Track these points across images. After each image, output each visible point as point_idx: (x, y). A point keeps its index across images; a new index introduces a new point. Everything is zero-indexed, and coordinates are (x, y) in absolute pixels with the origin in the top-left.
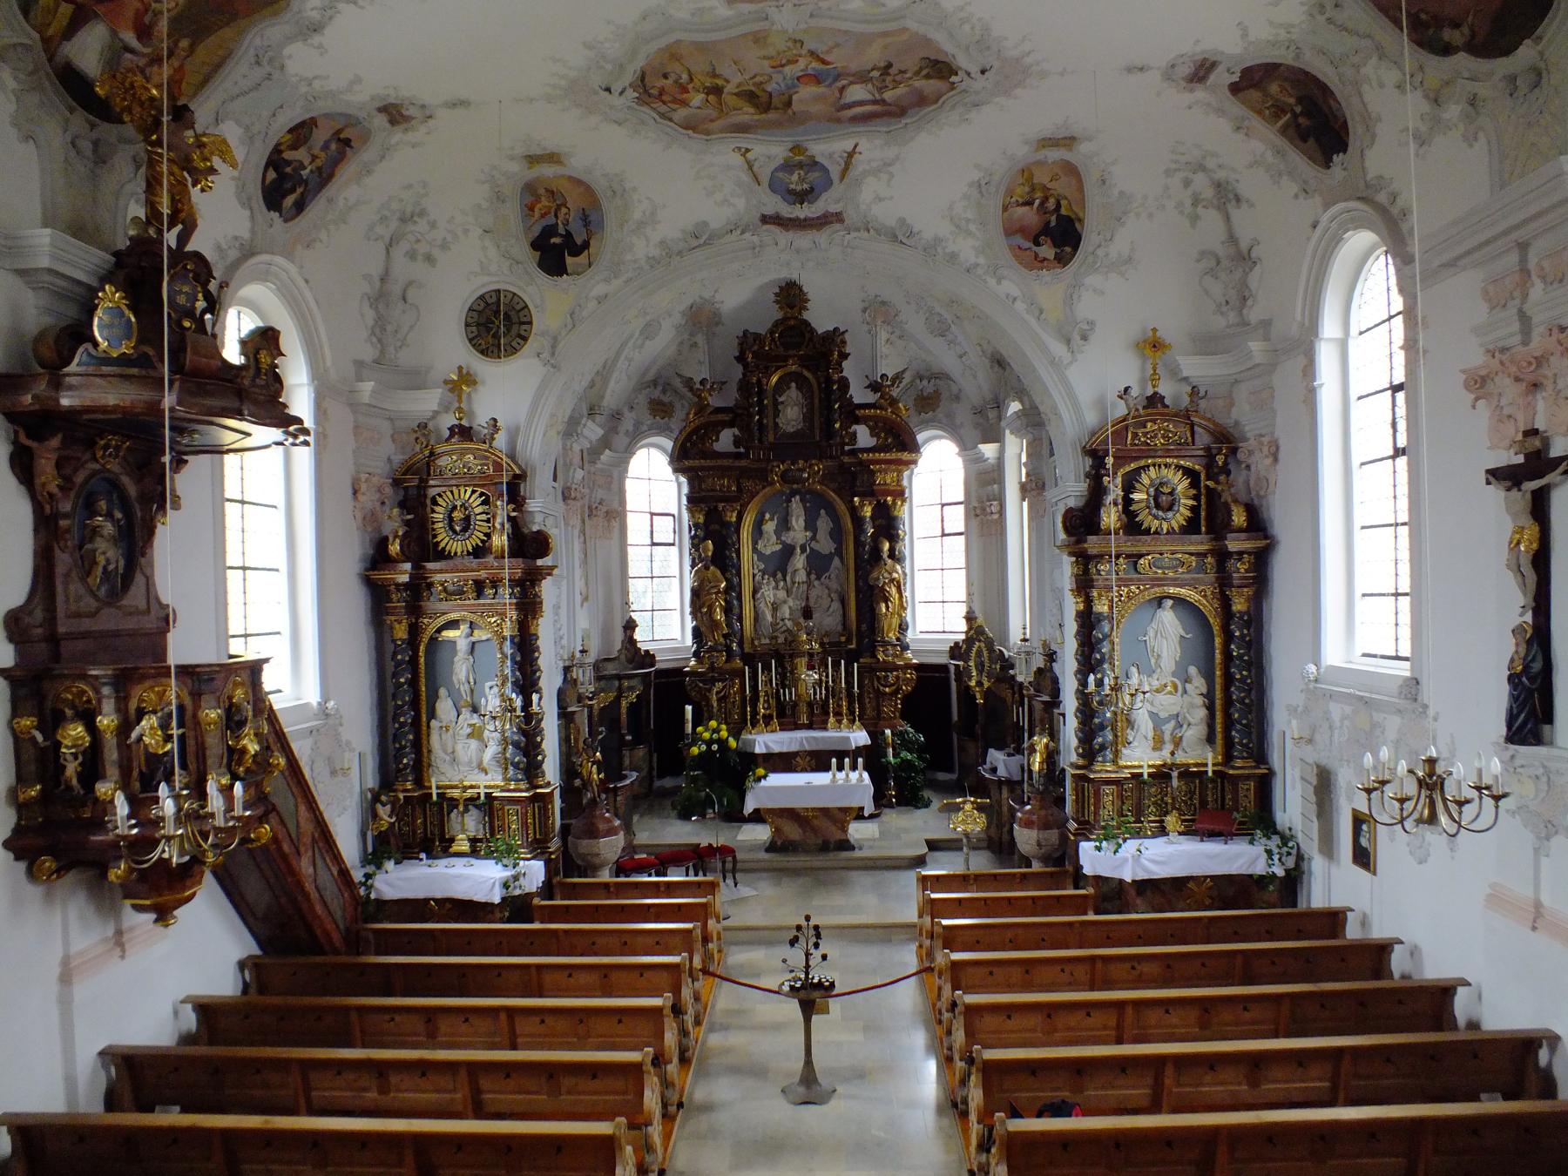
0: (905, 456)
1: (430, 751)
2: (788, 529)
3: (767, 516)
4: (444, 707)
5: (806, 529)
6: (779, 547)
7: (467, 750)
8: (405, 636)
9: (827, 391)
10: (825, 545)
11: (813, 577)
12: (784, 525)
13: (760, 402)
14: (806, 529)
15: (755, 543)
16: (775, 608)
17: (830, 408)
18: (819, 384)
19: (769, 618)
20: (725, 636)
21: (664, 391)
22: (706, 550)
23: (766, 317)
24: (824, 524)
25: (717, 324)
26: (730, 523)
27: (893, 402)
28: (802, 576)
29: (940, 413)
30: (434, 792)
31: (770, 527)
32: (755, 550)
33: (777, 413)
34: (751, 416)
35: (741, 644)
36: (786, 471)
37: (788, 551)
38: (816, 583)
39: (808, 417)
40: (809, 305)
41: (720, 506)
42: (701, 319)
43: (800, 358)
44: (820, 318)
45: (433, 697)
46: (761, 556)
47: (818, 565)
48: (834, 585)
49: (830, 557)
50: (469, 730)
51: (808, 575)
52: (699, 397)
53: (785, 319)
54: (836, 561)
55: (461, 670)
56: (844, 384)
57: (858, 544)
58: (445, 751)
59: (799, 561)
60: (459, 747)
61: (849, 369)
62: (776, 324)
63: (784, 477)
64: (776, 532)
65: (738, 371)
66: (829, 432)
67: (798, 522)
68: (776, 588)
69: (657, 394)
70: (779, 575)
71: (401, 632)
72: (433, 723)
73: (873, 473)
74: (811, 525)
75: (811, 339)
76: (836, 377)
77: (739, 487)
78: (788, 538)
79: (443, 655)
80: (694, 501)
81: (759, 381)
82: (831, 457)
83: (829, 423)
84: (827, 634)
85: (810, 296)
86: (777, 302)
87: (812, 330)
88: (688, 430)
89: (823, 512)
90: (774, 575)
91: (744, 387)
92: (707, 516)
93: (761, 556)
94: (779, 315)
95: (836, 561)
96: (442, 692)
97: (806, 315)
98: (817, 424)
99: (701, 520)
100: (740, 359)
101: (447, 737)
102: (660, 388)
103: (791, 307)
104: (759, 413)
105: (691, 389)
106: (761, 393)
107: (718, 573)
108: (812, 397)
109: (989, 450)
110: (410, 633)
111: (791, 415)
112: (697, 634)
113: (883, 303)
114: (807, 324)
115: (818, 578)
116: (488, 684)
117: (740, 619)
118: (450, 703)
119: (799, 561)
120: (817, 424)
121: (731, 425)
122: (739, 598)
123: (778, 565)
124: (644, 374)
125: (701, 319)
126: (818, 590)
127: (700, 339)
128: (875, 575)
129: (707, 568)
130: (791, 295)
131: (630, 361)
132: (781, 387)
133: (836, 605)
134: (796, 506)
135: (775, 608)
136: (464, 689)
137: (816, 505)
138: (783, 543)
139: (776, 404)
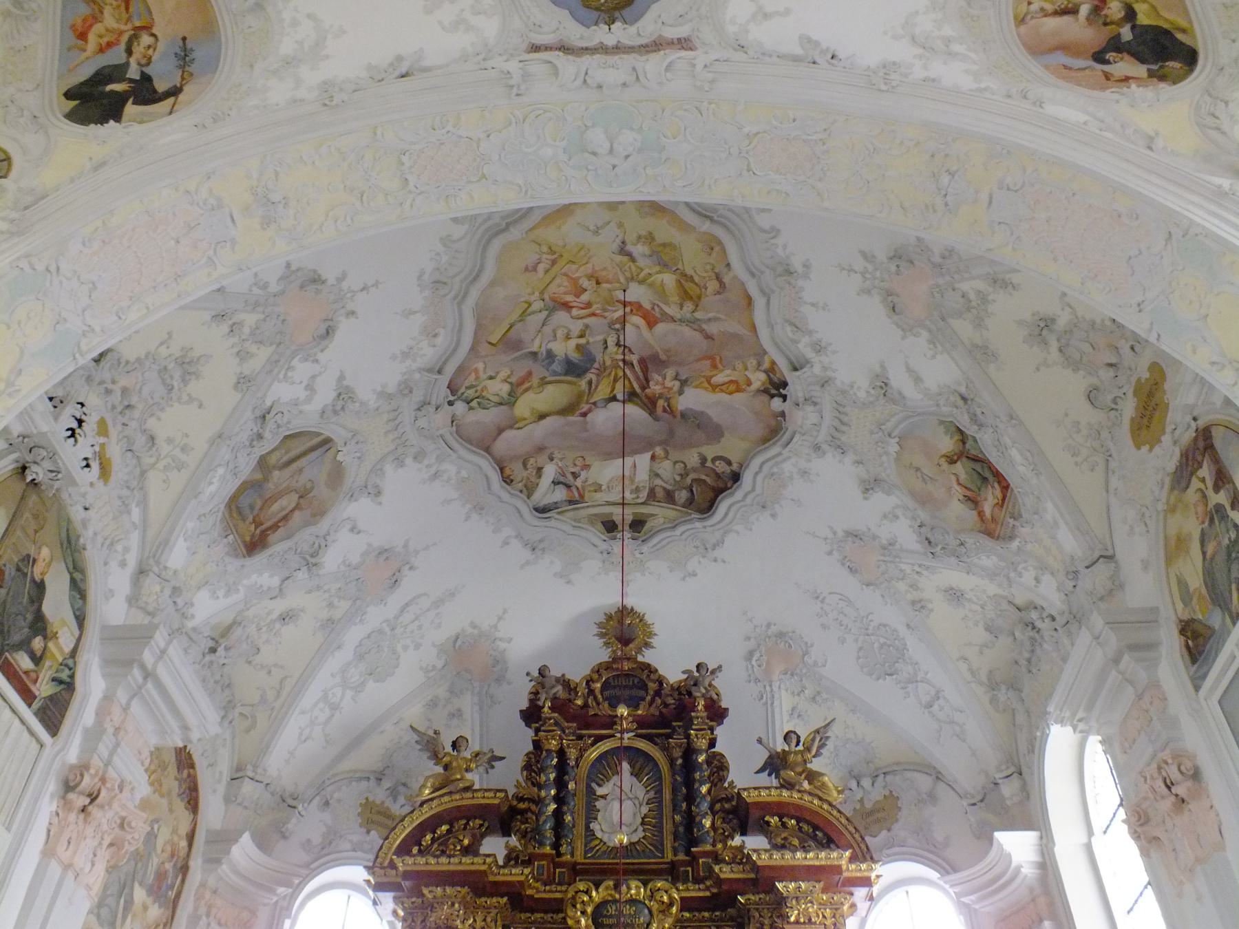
0: (840, 858)
9: (689, 765)
13: (560, 784)
17: (691, 798)
18: (672, 762)
21: (393, 793)
23: (581, 658)
25: (499, 680)
27: (812, 776)
29: (900, 830)
33: (591, 814)
34: (539, 801)
36: (600, 908)
39: (652, 822)
40: (654, 641)
42: (469, 662)
43: (641, 723)
44: (669, 661)
52: (446, 767)
53: (615, 660)
56: (719, 766)
61: (728, 740)
62: (598, 670)
65: (523, 738)
66: (689, 834)
69: (379, 795)
73: (780, 902)
75: (658, 693)
76: (702, 743)
81: (561, 753)
82: (697, 881)
83: (690, 821)
85: (656, 629)
86: (602, 635)
87: (660, 681)
91: (533, 765)
94: (604, 655)
97: (647, 657)
98: (668, 827)
100: (531, 715)
102: (386, 784)
103: (625, 641)
105: (436, 756)
106: (562, 768)
108: (659, 791)
109: (1017, 846)
111: (621, 813)
113: (781, 635)
114: (648, 669)
120: (668, 827)
124: (355, 743)
125: (469, 662)
127: (467, 703)
130: (624, 628)
131: (334, 707)
132: (605, 767)
139: (591, 795)
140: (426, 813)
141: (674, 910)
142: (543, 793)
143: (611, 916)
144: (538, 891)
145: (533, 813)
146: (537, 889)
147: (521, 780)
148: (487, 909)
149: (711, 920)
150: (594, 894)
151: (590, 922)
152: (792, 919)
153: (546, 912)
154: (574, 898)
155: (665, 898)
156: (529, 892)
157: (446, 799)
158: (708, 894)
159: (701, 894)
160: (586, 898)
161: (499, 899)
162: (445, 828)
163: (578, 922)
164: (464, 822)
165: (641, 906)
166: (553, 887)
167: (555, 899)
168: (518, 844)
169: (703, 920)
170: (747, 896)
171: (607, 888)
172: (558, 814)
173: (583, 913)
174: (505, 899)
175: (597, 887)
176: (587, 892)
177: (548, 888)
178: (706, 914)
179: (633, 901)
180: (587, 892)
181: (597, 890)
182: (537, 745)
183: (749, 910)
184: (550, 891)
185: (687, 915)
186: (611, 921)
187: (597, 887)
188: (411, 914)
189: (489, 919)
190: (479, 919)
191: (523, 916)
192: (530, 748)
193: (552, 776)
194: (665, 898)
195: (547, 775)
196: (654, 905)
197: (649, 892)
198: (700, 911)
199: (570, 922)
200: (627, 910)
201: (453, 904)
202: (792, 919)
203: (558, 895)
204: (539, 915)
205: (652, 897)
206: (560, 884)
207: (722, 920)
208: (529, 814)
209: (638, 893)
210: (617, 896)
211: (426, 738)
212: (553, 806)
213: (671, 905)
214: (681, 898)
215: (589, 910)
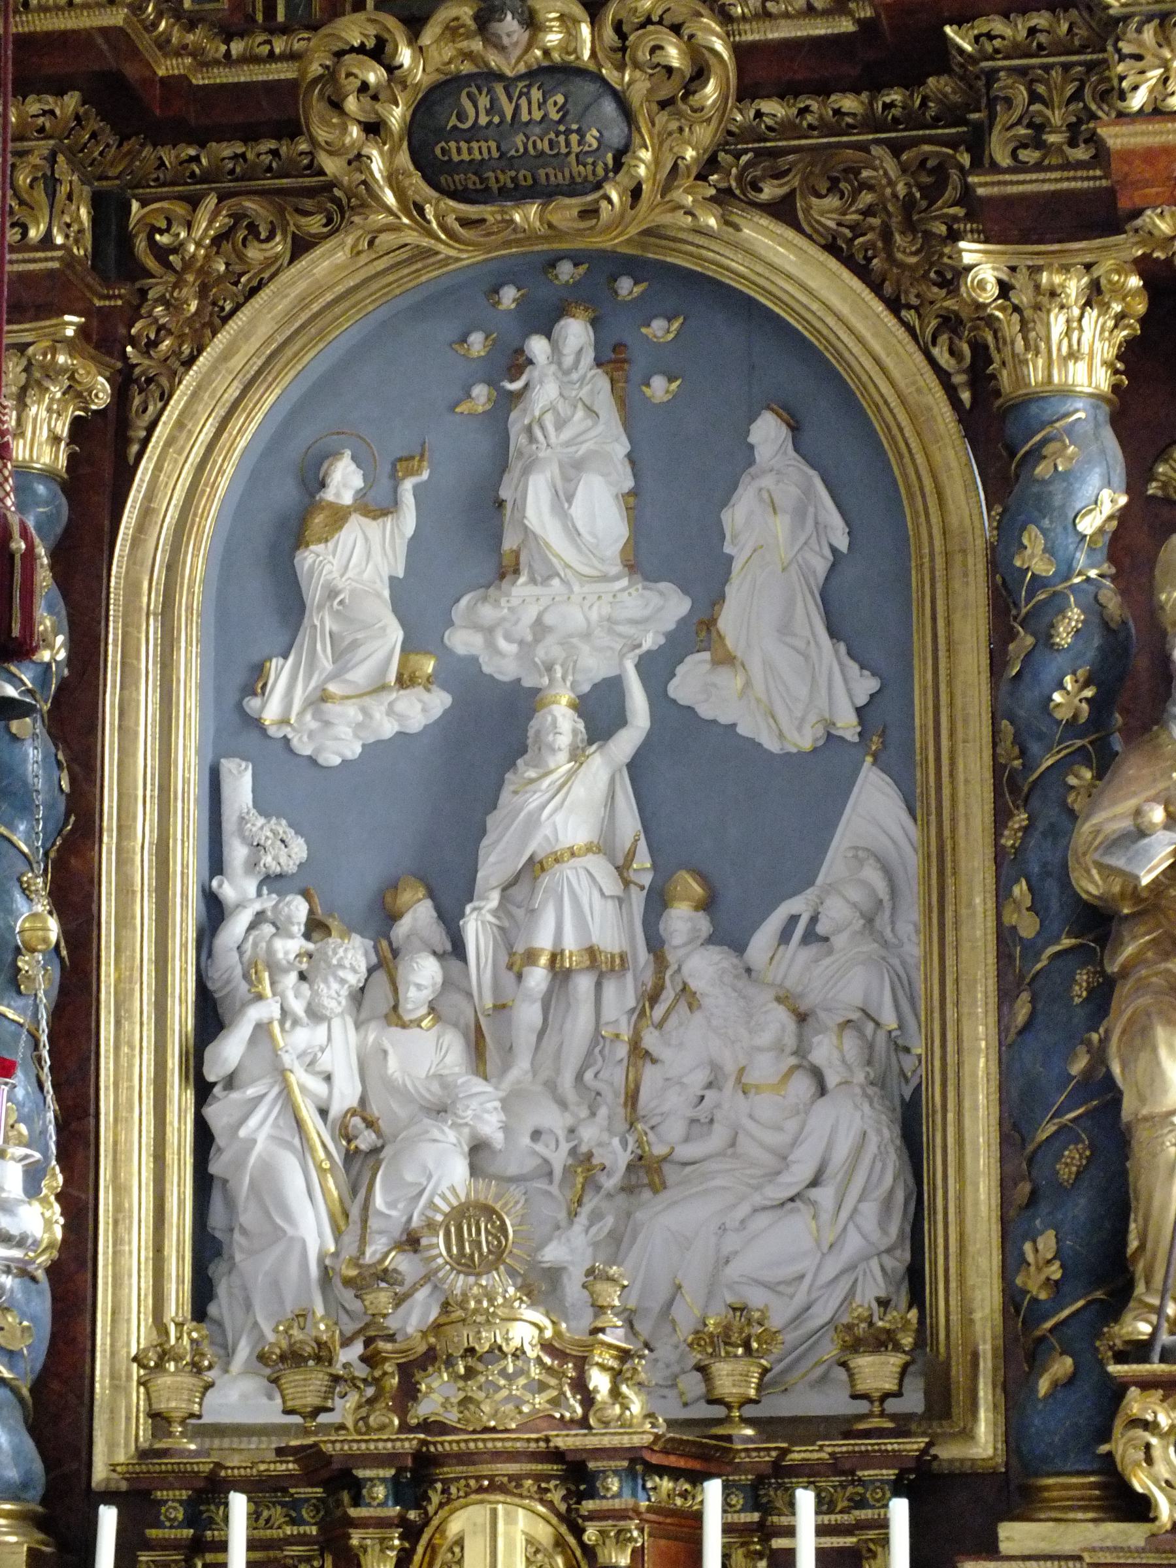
2: (506, 570)
3: (345, 480)
5: (639, 562)
6: (421, 709)
10: (784, 682)
11: (682, 920)
12: (477, 538)
14: (639, 562)
16: (361, 1159)
24: (780, 520)
28: (585, 911)
31: (358, 561)
32: (236, 724)
37: (490, 732)
38: (703, 967)
46: (290, 781)
47: (722, 826)
48: (849, 980)
49: (822, 776)
51: (658, 901)
54: (874, 806)
57: (1014, 606)
59: (570, 801)
63: (428, 144)
64: (403, 597)
67: (576, 497)
68: (379, 1000)
70: (419, 916)
74: (675, 539)
78: (494, 634)
84: (739, 1333)
89: (768, 433)
90: (381, 918)
93: (290, 781)
95: (874, 806)
115: (730, 936)
119: (570, 801)
123: (419, 844)
126: (724, 1024)
128: (1109, 817)
133: (850, 1128)
134: (563, 371)
135: (361, 1159)
137: (714, 366)
138: (463, 678)
141: (711, 91)
143: (474, 133)
144: (203, 62)
146: (196, 53)
149: (871, 123)
150: (405, 56)
151: (404, 159)
152: (1137, 101)
153: (250, 135)
154: (330, 76)
155: (674, 55)
156: (165, 68)
158: (846, 26)
159: (819, 29)
160: (374, 75)
161: (50, 102)
163: (358, 160)
165: (590, 88)
166: (257, 43)
167: (270, 87)
169: (837, 124)
170: (982, 26)
171: (453, 31)
173: (374, 128)
174: (72, 101)
175: (414, 25)
176: (379, 52)
177: (237, 47)
178: (849, 103)
179: (557, 73)
180: (379, 52)
181: (413, 38)
183: (991, 76)
184: (250, 59)
185: (774, 108)
186: (479, 150)
187: (414, 25)
191: (169, 156)
194: (674, 55)
196: (636, 84)
197: (609, 34)
198: (823, 90)
199: (331, 166)
200: (535, 106)
202: (1137, 101)
203: (283, 72)
204: (227, 150)
205: (622, 52)
206: (273, 29)
207: (912, 119)
209: (570, 44)
210: (494, 60)
213: (700, 75)
214: (739, 50)
215: (396, 116)
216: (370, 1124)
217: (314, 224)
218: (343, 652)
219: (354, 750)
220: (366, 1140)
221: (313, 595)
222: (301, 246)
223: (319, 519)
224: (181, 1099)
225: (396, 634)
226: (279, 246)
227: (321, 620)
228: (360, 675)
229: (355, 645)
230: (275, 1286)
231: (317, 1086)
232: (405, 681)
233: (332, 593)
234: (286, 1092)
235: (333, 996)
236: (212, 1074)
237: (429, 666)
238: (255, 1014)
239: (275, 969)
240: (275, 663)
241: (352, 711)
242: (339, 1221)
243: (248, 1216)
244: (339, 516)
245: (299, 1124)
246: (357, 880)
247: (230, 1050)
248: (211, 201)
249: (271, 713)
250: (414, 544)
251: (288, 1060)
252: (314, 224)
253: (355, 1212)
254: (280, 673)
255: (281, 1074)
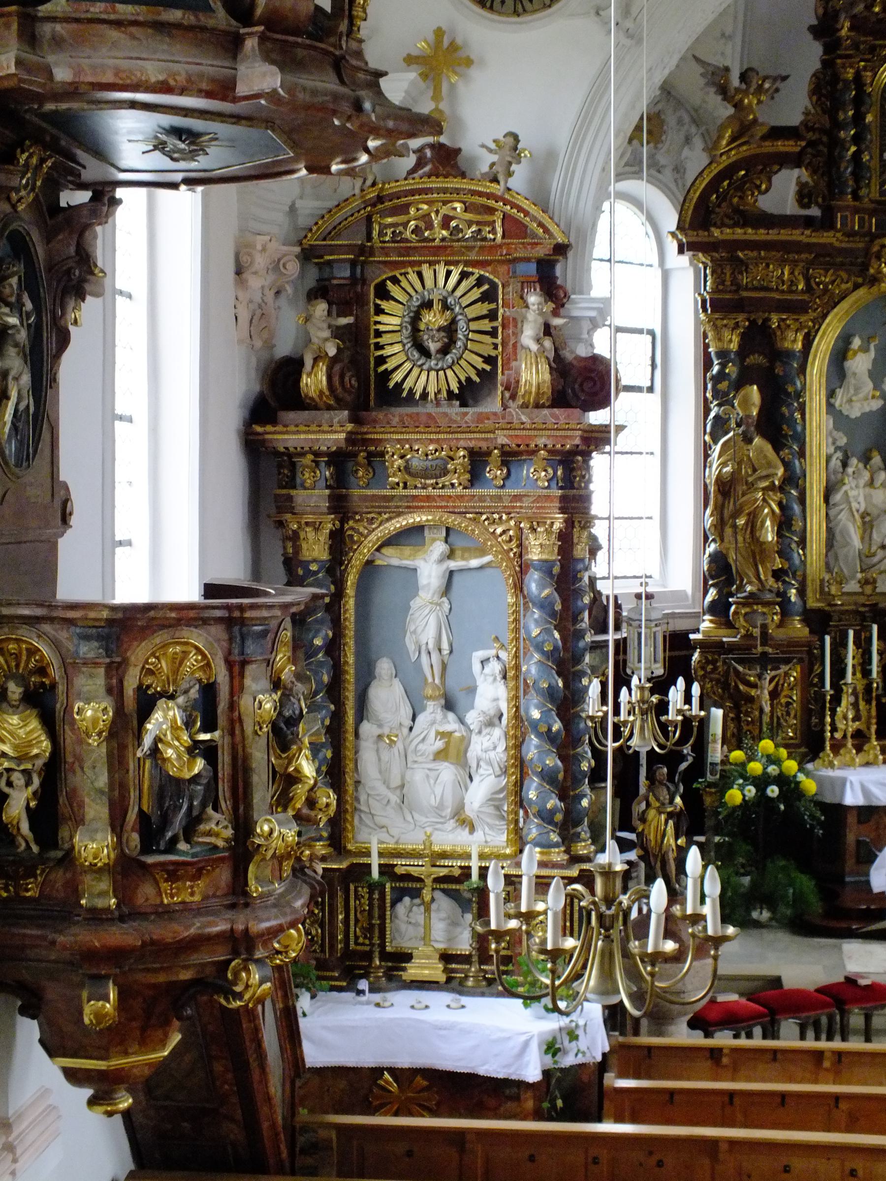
1: (358, 783)
3: (856, 342)
4: (387, 697)
7: (435, 783)
8: (325, 556)
13: (858, 118)
15: (831, 394)
19: (856, 542)
20: (778, 575)
22: (745, 403)
26: (790, 354)
30: (375, 862)
32: (830, 406)
35: (802, 592)
41: (775, 319)
45: (367, 676)
50: (439, 744)
55: (424, 624)
58: (386, 783)
60: (417, 776)
64: (872, 374)
71: (315, 548)
72: (366, 728)
77: (807, 280)
79: (384, 596)
80: (720, 305)
88: (716, 169)
92: (745, 338)
96: (384, 667)
99: (734, 346)
101: (393, 757)
104: (857, 139)
105: (723, 91)
107: (768, 448)
110: (332, 550)
112: (720, 572)
116: (478, 656)
117: (802, 543)
118: (398, 688)
121: (795, 160)
122: (802, 500)
129: (748, 440)
136: (429, 665)
140: (725, 161)
142: (842, 134)
145: (822, 143)
147: (810, 107)
148: (794, 263)
157: (745, 148)
162: (743, 173)
164: (760, 167)
168: (809, 180)
172: (857, 156)
182: (827, 64)
188: (720, 265)
189: (796, 273)
190: (786, 273)
192: (818, 65)
193: (851, 113)
195: (846, 113)
201: (768, 266)
208: (821, 147)
211: (711, 69)
212: (853, 149)
216: (868, 514)
217: (860, 280)
218: (857, 390)
219: (858, 414)
220: (868, 519)
221: (849, 373)
222: (856, 287)
223: (851, 353)
224: (823, 506)
225: (871, 385)
226: (849, 285)
227: (851, 381)
228: (861, 396)
229: (860, 388)
230: (846, 556)
231: (857, 506)
232: (873, 397)
233: (855, 374)
234: (851, 509)
235: (862, 482)
236: (832, 502)
237: (878, 394)
238: (845, 488)
239: (848, 476)
240: (838, 390)
241: (858, 405)
242: (862, 539)
243: (838, 537)
244: (855, 353)
245: (853, 516)
246: (860, 448)
247: (837, 497)
248: (831, 271)
249: (837, 404)
250: (875, 361)
251: (852, 499)
252: (860, 280)
253: (867, 538)
254: (839, 392)
255: (849, 503)
